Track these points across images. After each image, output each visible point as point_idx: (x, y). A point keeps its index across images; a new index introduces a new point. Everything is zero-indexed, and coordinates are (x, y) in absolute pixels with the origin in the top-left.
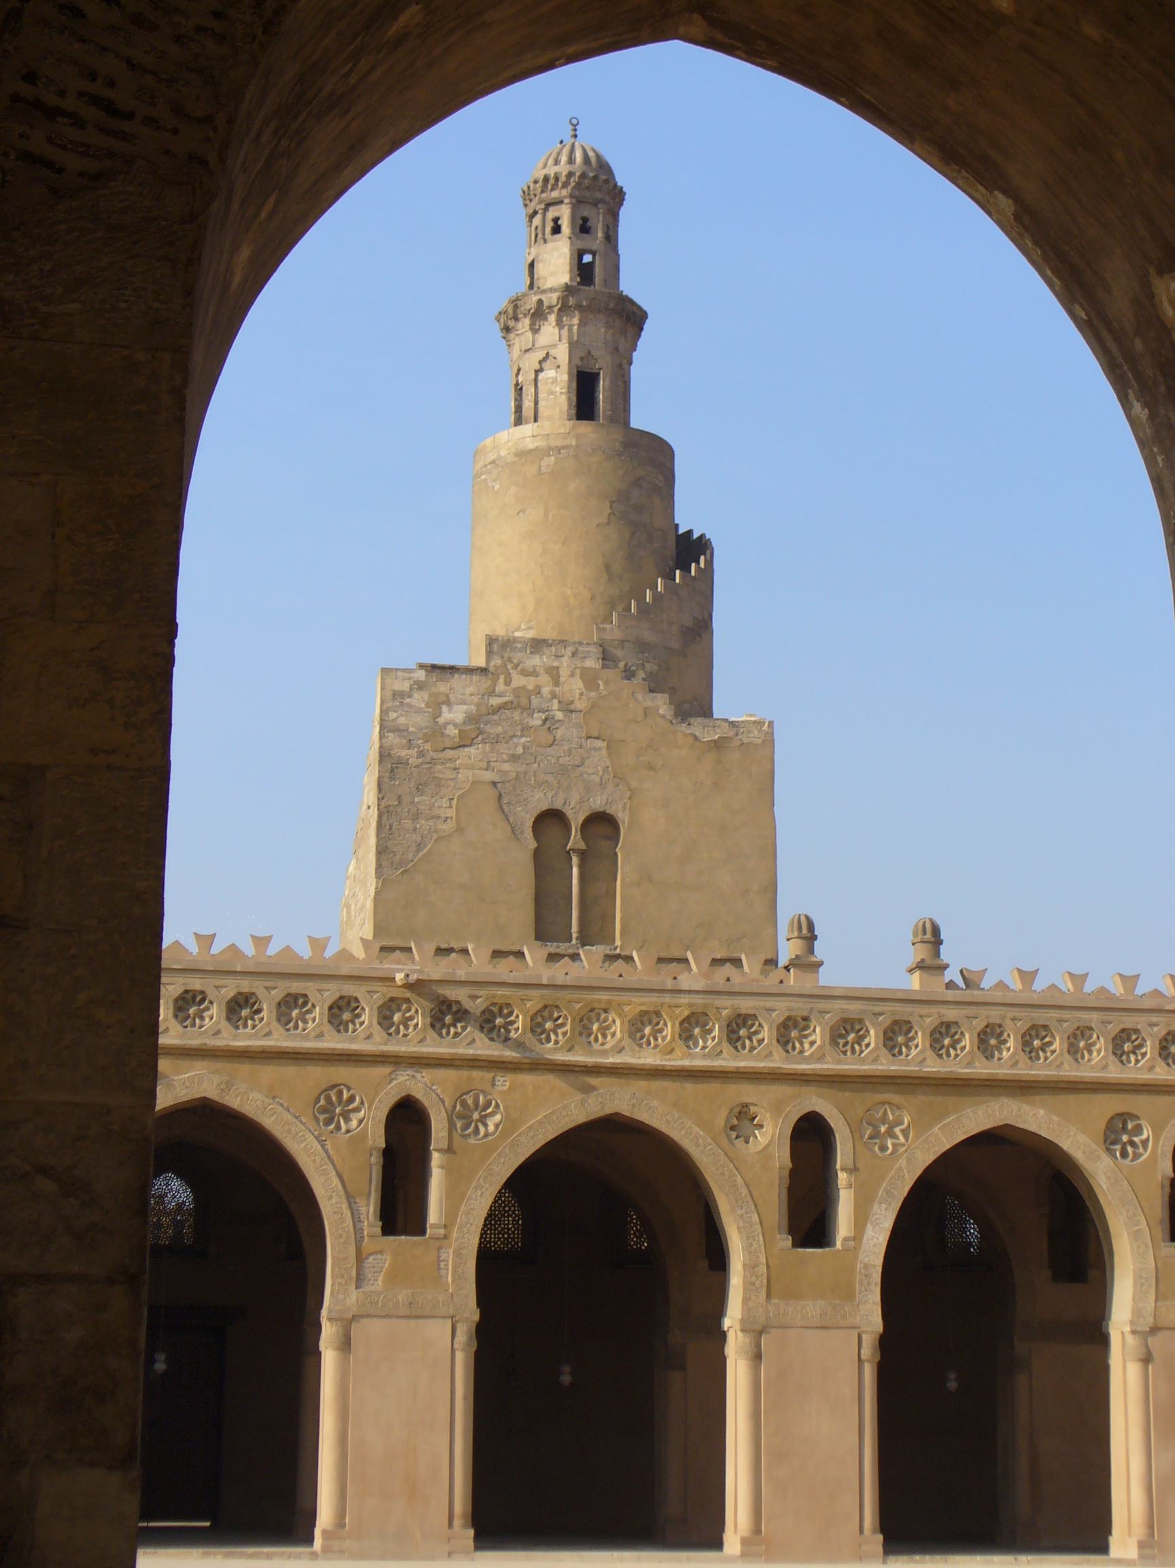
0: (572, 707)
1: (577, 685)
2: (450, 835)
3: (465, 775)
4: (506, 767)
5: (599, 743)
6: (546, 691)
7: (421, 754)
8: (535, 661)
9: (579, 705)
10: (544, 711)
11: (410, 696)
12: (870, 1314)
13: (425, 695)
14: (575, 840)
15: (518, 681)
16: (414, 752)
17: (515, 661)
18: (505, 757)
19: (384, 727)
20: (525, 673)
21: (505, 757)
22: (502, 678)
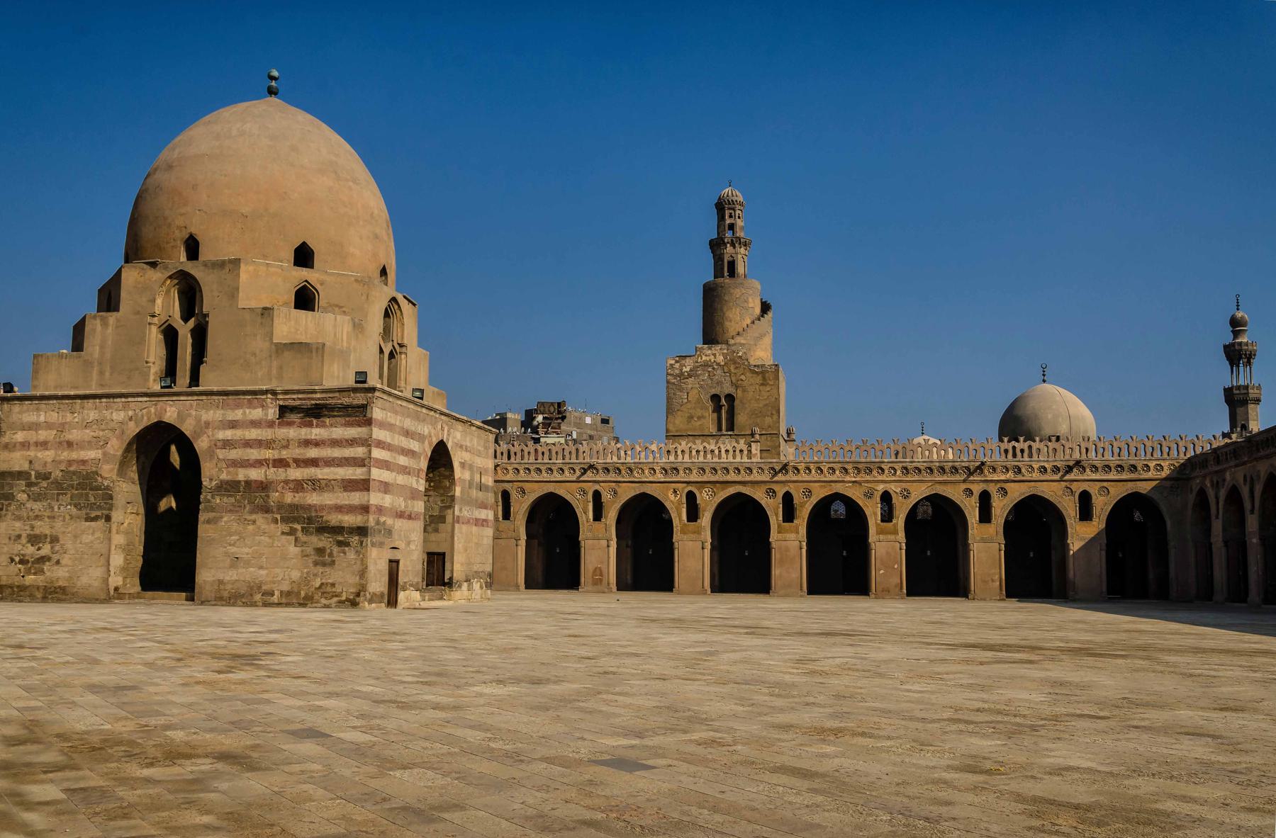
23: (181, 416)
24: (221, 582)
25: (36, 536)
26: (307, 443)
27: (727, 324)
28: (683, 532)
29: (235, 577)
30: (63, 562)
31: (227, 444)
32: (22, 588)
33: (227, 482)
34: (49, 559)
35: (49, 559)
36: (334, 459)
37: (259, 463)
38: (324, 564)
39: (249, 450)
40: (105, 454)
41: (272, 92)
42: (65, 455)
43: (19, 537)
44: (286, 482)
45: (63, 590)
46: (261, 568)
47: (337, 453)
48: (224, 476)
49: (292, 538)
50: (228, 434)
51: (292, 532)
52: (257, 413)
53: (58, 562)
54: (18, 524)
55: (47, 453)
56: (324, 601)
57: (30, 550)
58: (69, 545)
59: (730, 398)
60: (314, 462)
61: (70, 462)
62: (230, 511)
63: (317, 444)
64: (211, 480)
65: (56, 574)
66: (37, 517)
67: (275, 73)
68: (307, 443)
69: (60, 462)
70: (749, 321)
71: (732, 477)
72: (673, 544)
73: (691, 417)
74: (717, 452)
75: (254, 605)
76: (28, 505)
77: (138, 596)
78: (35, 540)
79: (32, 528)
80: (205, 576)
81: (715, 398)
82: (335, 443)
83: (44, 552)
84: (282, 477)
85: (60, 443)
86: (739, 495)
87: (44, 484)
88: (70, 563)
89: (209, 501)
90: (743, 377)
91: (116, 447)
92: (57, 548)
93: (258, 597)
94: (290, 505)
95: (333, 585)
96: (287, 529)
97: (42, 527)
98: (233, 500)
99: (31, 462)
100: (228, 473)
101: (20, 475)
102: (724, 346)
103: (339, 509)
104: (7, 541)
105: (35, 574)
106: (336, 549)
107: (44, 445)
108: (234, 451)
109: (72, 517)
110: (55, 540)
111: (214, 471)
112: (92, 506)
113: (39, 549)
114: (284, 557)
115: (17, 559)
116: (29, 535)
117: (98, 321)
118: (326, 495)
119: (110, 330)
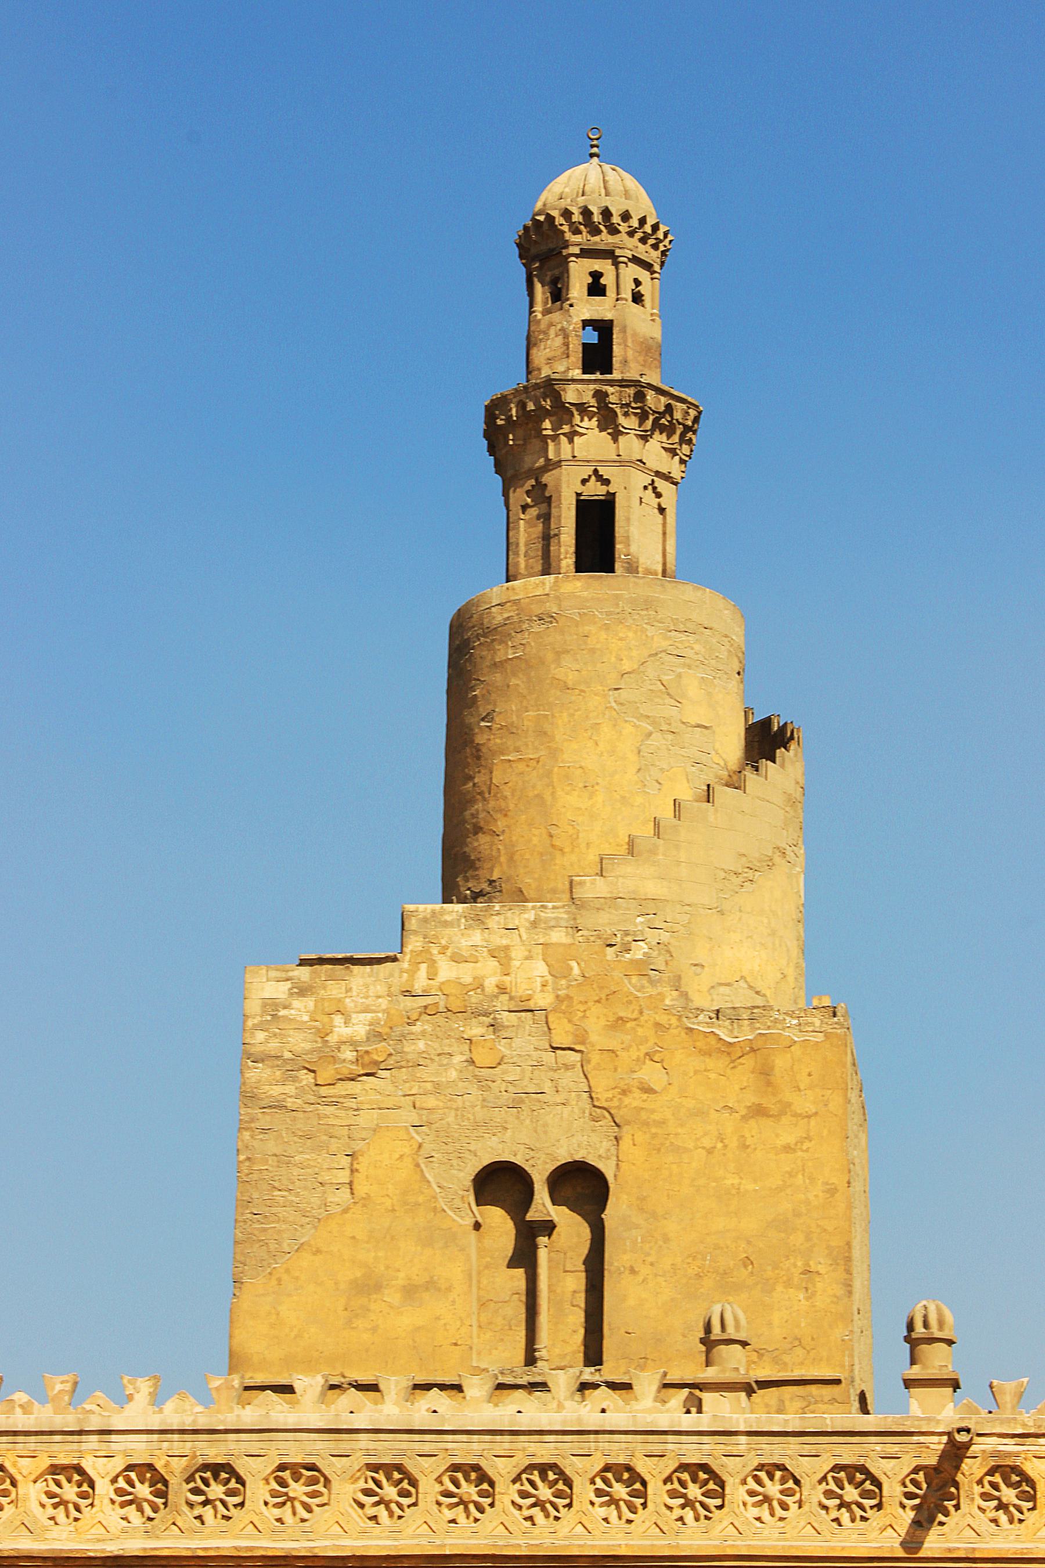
0: (531, 1005)
1: (540, 968)
2: (346, 1211)
3: (367, 1119)
4: (431, 1102)
5: (574, 1057)
6: (490, 984)
7: (301, 1091)
8: (477, 937)
9: (543, 1000)
10: (486, 1014)
11: (285, 1007)
13: (309, 1002)
15: (446, 971)
16: (290, 1089)
17: (443, 942)
18: (429, 1086)
20: (457, 959)
21: (429, 1086)
22: (423, 967)
27: (569, 802)
59: (583, 1186)
70: (685, 793)
73: (368, 1286)
102: (555, 911)
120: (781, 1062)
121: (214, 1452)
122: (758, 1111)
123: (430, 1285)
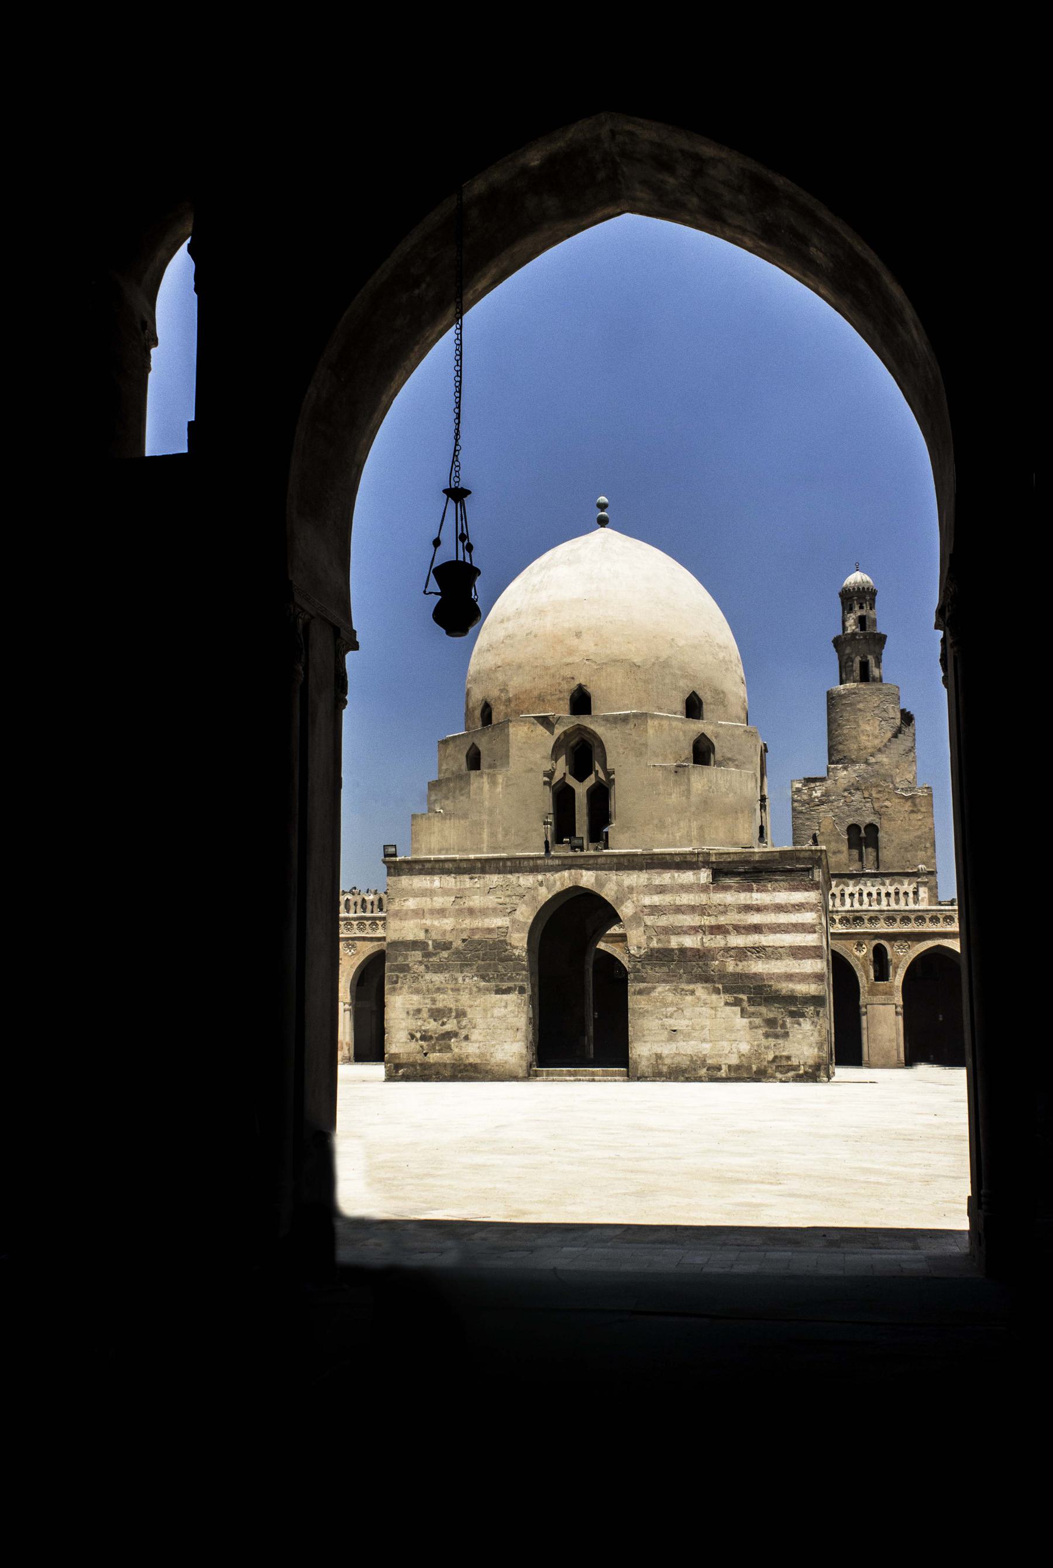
12: (898, 999)
14: (863, 834)
19: (794, 801)
23: (600, 883)
24: (659, 1057)
25: (438, 1010)
26: (748, 908)
28: (872, 992)
29: (674, 1051)
30: (473, 1037)
31: (655, 910)
32: (425, 1066)
33: (658, 950)
34: (455, 1035)
35: (455, 1035)
36: (779, 925)
37: (695, 930)
38: (776, 1036)
39: (681, 917)
40: (513, 922)
41: (603, 522)
42: (468, 923)
43: (419, 1011)
44: (727, 949)
45: (474, 1067)
46: (704, 1041)
47: (783, 918)
48: (654, 944)
49: (738, 1009)
50: (656, 899)
51: (737, 1003)
52: (687, 877)
53: (466, 1038)
54: (416, 998)
55: (446, 921)
56: (778, 1075)
57: (432, 1026)
58: (479, 1021)
59: (873, 829)
60: (757, 929)
61: (473, 931)
62: (664, 981)
63: (758, 909)
64: (639, 948)
65: (470, 1050)
66: (438, 990)
67: (603, 499)
68: (748, 908)
69: (462, 931)
71: (929, 927)
72: (858, 1007)
74: (875, 896)
75: (699, 1079)
76: (428, 976)
77: (529, 1076)
78: (437, 1014)
79: (434, 1001)
80: (641, 1050)
81: (853, 829)
82: (780, 908)
83: (448, 1027)
84: (722, 944)
85: (458, 910)
86: (939, 946)
87: (445, 954)
88: (480, 1038)
89: (639, 971)
90: (887, 803)
91: (526, 914)
92: (464, 1023)
93: (703, 1072)
94: (733, 975)
95: (788, 1058)
96: (731, 999)
97: (445, 1000)
98: (665, 969)
99: (427, 931)
100: (659, 941)
101: (415, 945)
103: (789, 977)
104: (404, 1015)
105: (440, 1051)
106: (788, 1020)
107: (442, 912)
108: (664, 918)
109: (479, 990)
110: (461, 1014)
111: (643, 940)
112: (501, 978)
113: (443, 1024)
114: (730, 1030)
115: (418, 1035)
116: (430, 1010)
117: (485, 779)
118: (773, 962)
119: (499, 789)
120: (918, 801)
121: (857, 914)
122: (912, 812)
123: (839, 852)
